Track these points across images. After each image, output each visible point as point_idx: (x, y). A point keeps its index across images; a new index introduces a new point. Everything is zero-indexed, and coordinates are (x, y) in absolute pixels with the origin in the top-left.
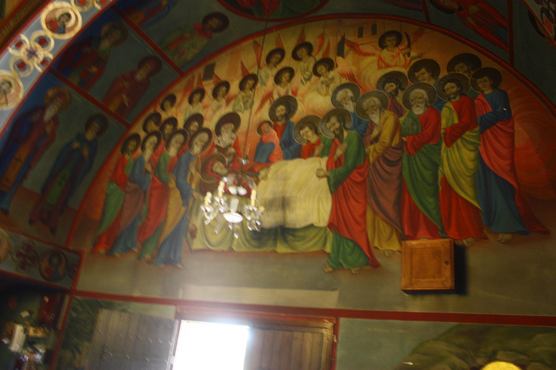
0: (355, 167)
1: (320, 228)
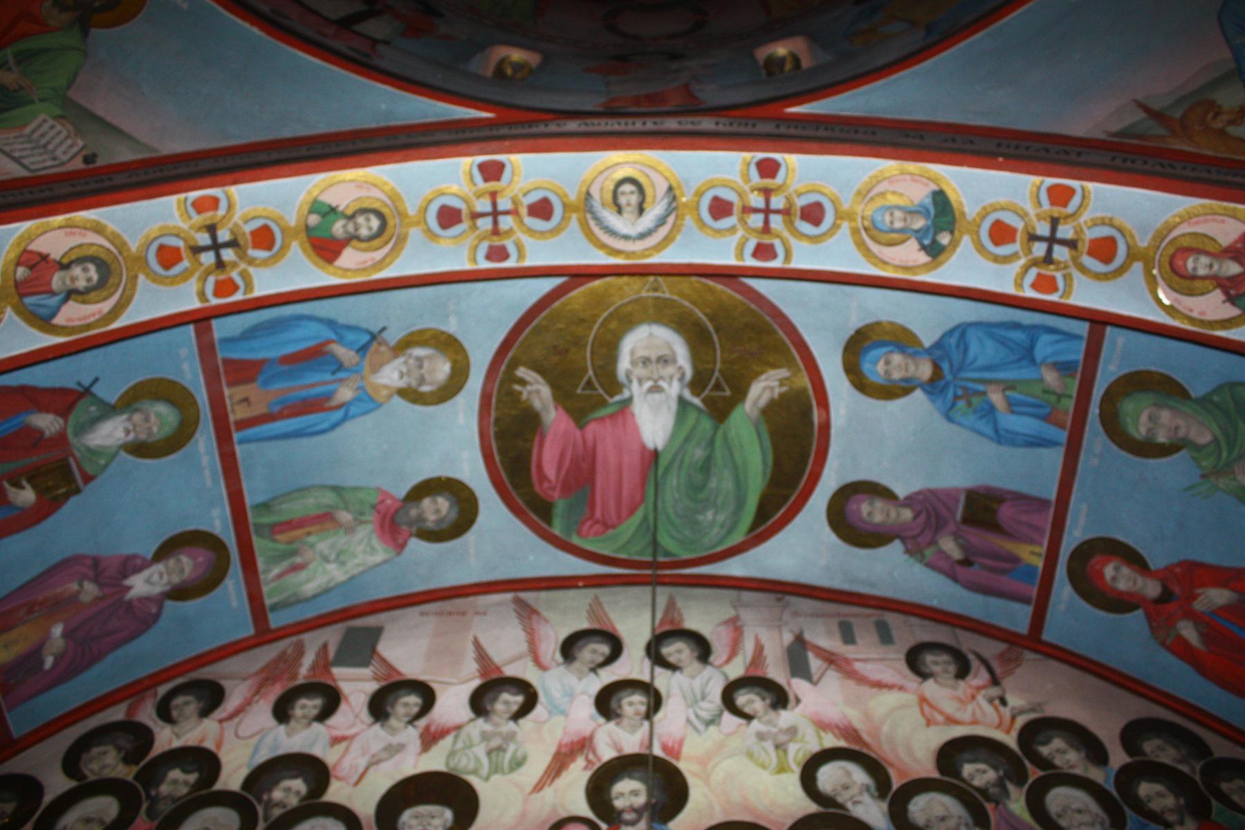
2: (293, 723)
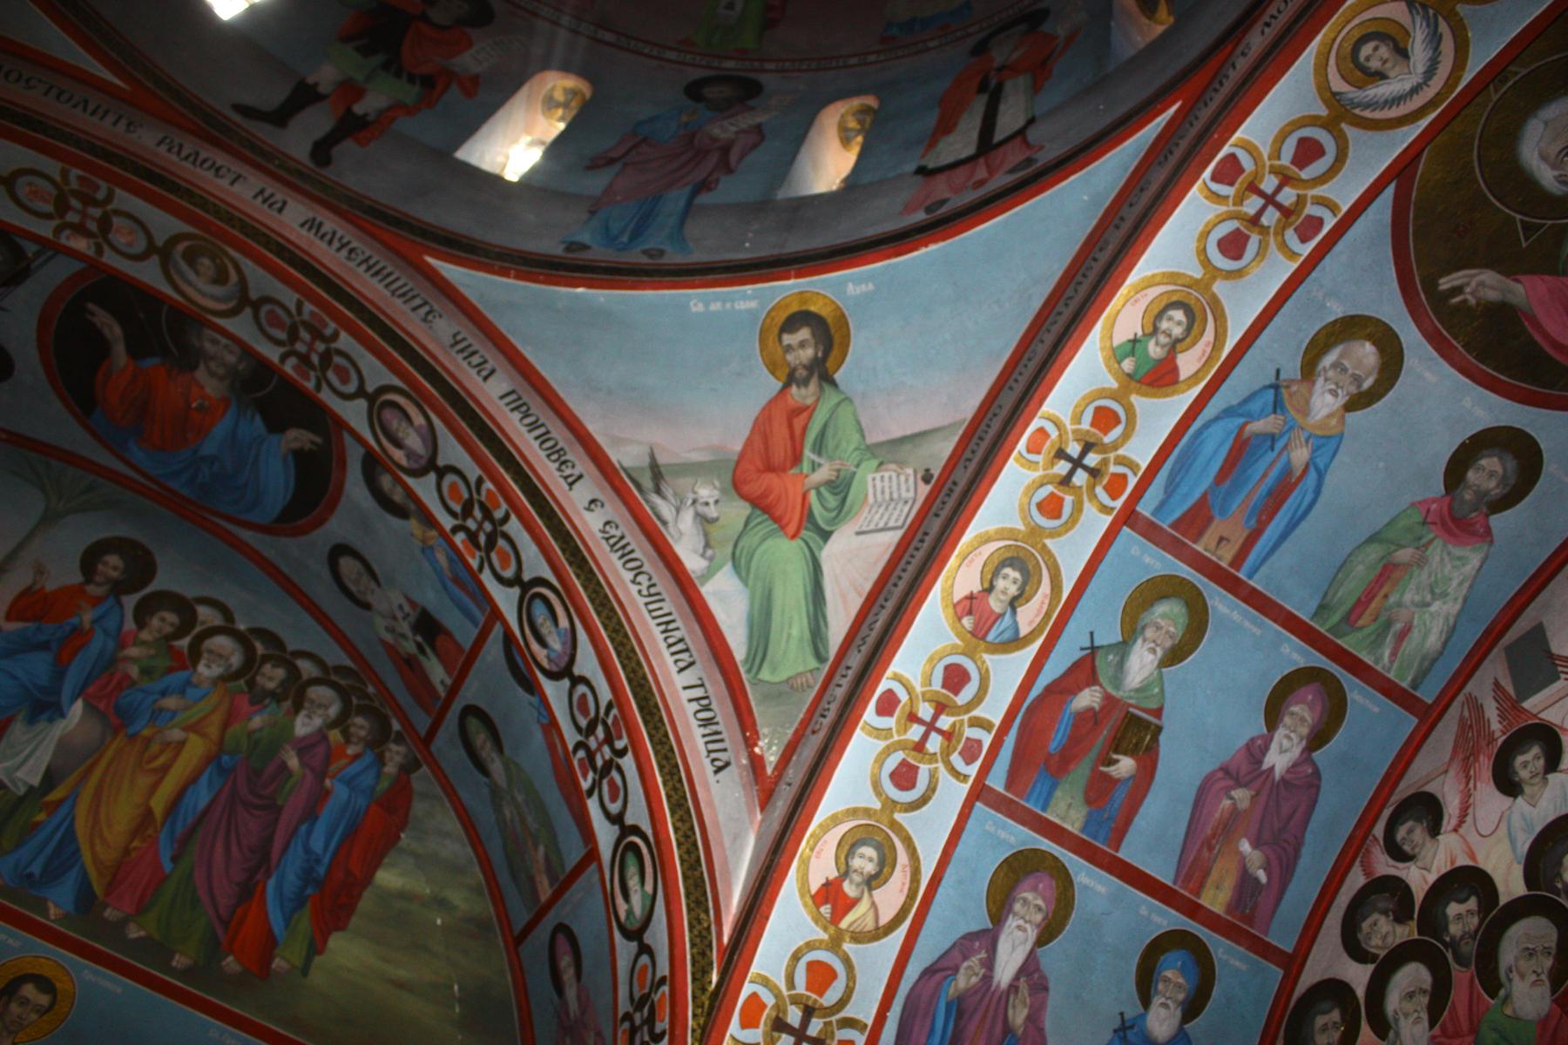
2: (1527, 789)
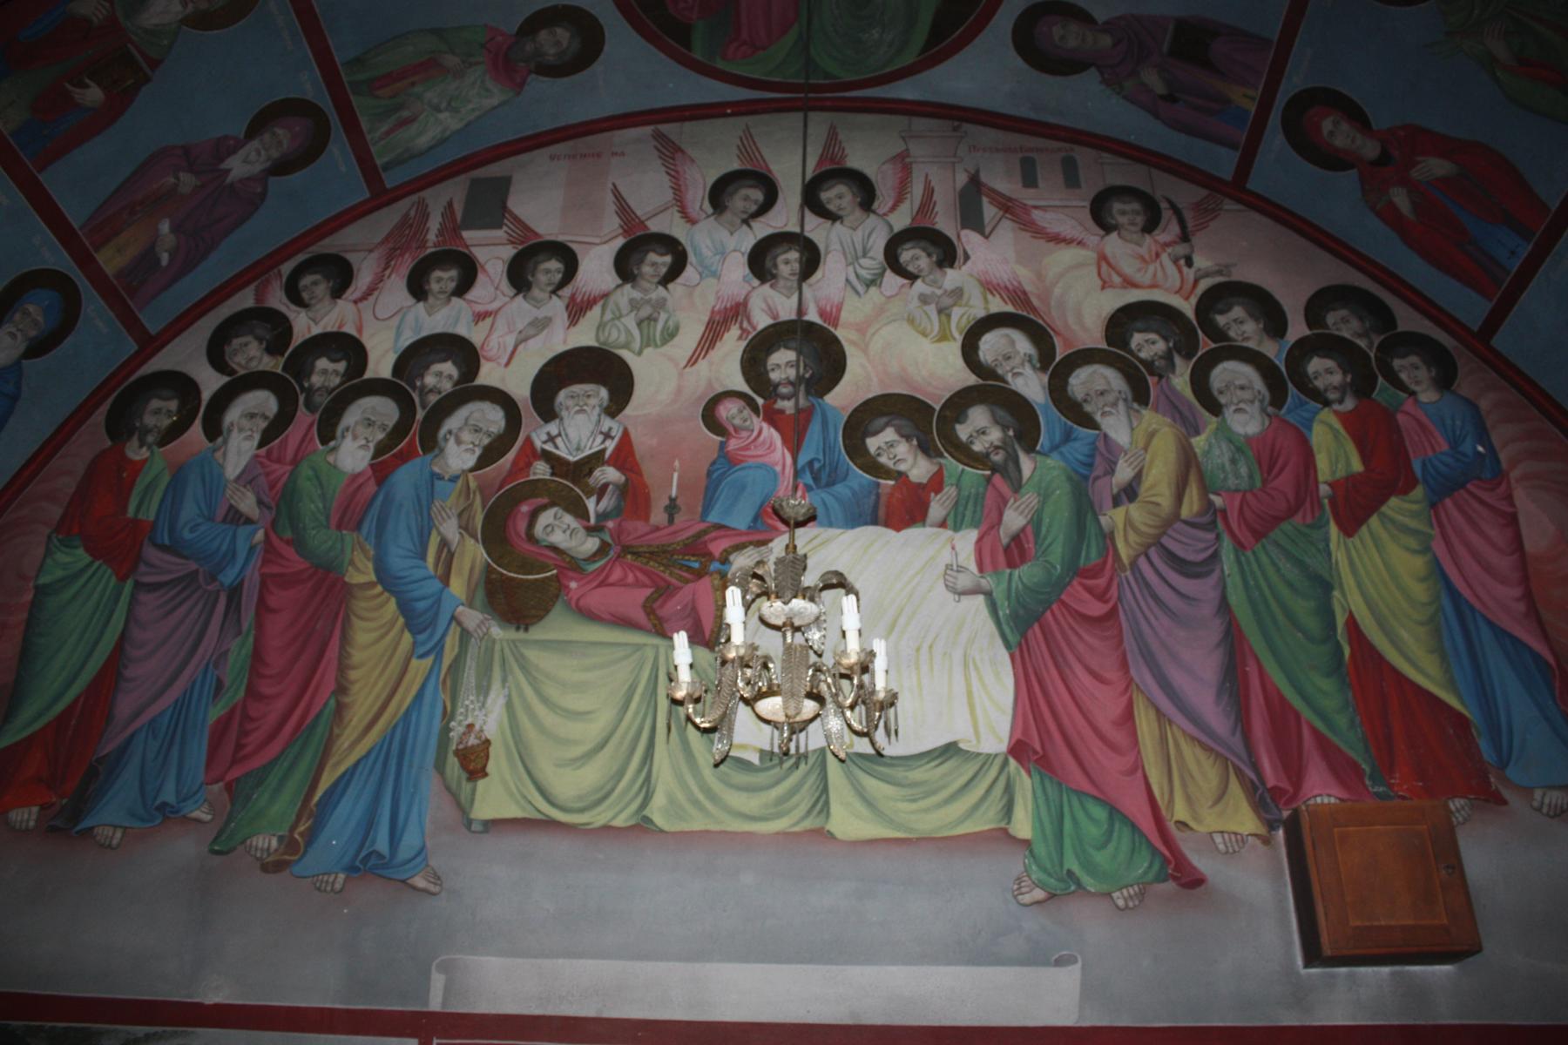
0: (1078, 571)
1: (989, 758)
2: (431, 300)
